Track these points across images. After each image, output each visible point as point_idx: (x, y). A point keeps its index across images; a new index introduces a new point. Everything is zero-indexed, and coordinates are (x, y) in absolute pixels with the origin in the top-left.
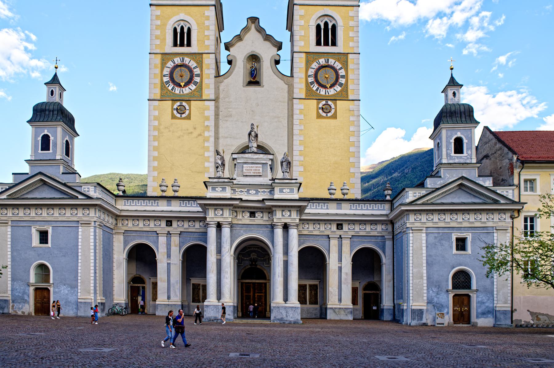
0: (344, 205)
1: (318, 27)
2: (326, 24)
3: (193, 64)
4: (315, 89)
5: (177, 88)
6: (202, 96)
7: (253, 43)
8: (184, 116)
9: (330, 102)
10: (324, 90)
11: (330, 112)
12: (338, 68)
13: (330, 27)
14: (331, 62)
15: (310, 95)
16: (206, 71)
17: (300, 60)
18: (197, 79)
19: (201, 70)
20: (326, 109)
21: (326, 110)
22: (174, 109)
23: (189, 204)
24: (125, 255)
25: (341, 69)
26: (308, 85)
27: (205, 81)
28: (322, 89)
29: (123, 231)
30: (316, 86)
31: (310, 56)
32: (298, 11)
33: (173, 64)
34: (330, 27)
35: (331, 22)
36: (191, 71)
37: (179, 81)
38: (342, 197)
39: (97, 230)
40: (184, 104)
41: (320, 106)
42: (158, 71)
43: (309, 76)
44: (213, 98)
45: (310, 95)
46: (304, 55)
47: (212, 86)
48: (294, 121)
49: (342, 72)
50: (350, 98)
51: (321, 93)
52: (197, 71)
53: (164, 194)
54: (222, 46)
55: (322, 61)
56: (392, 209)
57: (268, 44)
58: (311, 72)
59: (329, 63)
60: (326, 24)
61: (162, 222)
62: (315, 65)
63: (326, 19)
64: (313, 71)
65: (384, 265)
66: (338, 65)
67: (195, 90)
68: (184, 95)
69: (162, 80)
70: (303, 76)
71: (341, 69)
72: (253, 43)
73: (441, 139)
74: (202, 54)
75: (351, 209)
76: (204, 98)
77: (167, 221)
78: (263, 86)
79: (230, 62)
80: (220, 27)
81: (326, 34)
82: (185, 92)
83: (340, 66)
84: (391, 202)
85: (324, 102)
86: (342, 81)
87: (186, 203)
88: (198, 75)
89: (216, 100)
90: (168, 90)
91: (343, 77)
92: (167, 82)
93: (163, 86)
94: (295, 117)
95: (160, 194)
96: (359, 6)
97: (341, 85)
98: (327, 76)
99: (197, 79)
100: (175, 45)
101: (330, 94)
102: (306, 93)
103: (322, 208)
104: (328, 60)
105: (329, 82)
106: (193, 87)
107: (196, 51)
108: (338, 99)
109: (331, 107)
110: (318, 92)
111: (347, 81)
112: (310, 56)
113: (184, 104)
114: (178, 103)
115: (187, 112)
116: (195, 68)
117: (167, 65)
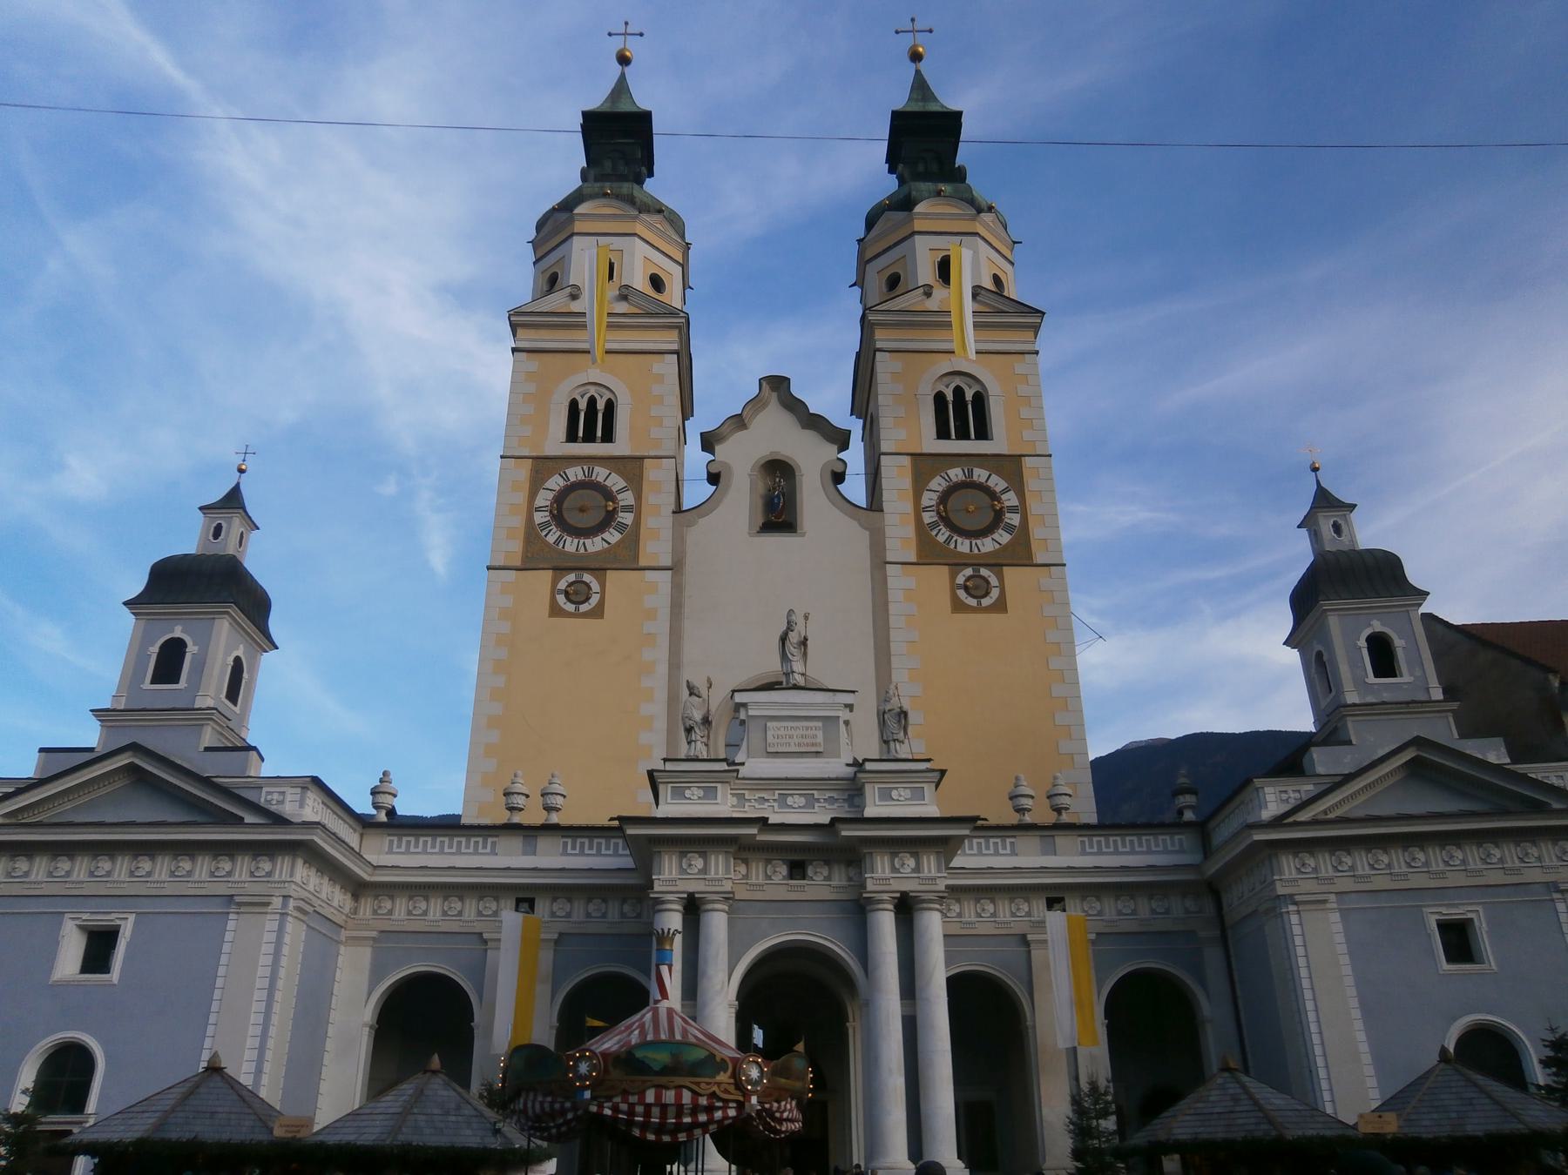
0: (1062, 841)
1: (939, 399)
2: (958, 392)
3: (615, 482)
4: (941, 539)
5: (569, 539)
6: (636, 557)
7: (775, 435)
8: (584, 608)
9: (984, 572)
10: (967, 542)
11: (987, 594)
12: (998, 489)
13: (969, 396)
14: (980, 475)
15: (929, 553)
16: (650, 498)
17: (897, 476)
18: (627, 518)
19: (638, 497)
20: (977, 588)
21: (976, 590)
22: (560, 592)
23: (591, 848)
24: (368, 1014)
25: (1005, 491)
27: (649, 522)
28: (960, 540)
29: (374, 934)
30: (943, 535)
31: (925, 465)
32: (885, 366)
33: (562, 483)
34: (969, 396)
36: (608, 495)
37: (576, 515)
38: (1051, 818)
39: (289, 927)
40: (587, 577)
41: (960, 580)
42: (521, 498)
43: (925, 509)
44: (667, 562)
45: (929, 553)
46: (906, 461)
47: (667, 534)
48: (892, 619)
49: (1010, 499)
50: (1039, 559)
51: (960, 548)
52: (627, 498)
53: (517, 818)
54: (694, 442)
55: (956, 474)
56: (1207, 850)
57: (811, 438)
58: (929, 499)
61: (502, 903)
62: (938, 484)
64: (935, 496)
65: (1209, 1029)
66: (997, 483)
67: (618, 543)
68: (588, 556)
69: (530, 519)
70: (908, 507)
71: (1005, 491)
72: (775, 435)
73: (1328, 642)
74: (643, 458)
75: (1084, 853)
76: (643, 562)
77: (519, 901)
78: (803, 535)
79: (714, 478)
80: (687, 410)
81: (963, 412)
82: (591, 549)
84: (1202, 829)
85: (969, 571)
86: (1014, 519)
87: (582, 845)
88: (628, 509)
89: (676, 568)
90: (547, 544)
91: (1013, 510)
92: (545, 525)
93: (532, 534)
94: (893, 608)
95: (502, 817)
96: (1037, 353)
97: (1009, 528)
98: (970, 509)
99: (627, 518)
100: (572, 437)
101: (984, 550)
102: (920, 553)
103: (997, 853)
104: (971, 472)
105: (979, 521)
106: (613, 536)
107: (627, 453)
109: (988, 582)
112: (925, 465)
113: (587, 577)
114: (572, 577)
115: (595, 599)
116: (620, 491)
117: (547, 485)
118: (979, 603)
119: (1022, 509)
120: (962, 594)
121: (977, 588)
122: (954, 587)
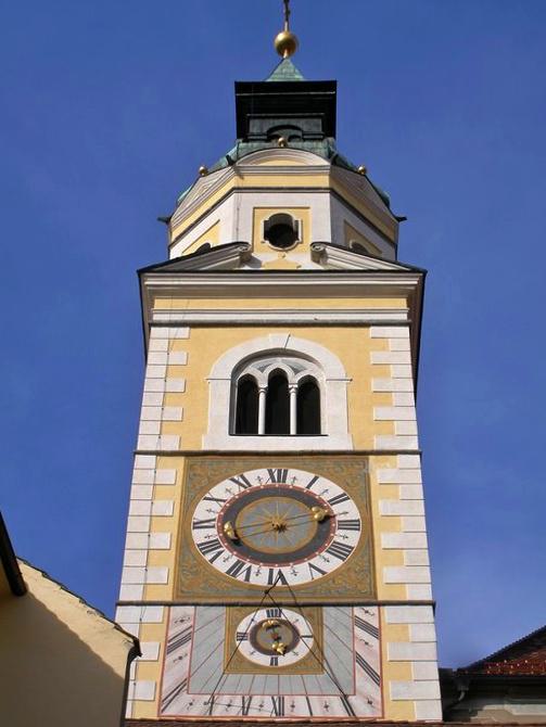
2: (278, 379)
9: (289, 615)
10: (265, 570)
12: (326, 498)
14: (299, 478)
26: (187, 554)
28: (255, 568)
30: (224, 561)
34: (294, 380)
35: (296, 371)
43: (199, 525)
51: (254, 580)
55: (258, 477)
59: (288, 482)
60: (278, 379)
63: (279, 363)
64: (217, 507)
66: (326, 488)
71: (337, 500)
83: (337, 490)
91: (350, 525)
97: (340, 551)
108: (326, 601)
110: (241, 577)
111: (368, 541)
118: (274, 662)
119: (366, 525)
120: (245, 648)
121: (276, 637)
122: (233, 636)
